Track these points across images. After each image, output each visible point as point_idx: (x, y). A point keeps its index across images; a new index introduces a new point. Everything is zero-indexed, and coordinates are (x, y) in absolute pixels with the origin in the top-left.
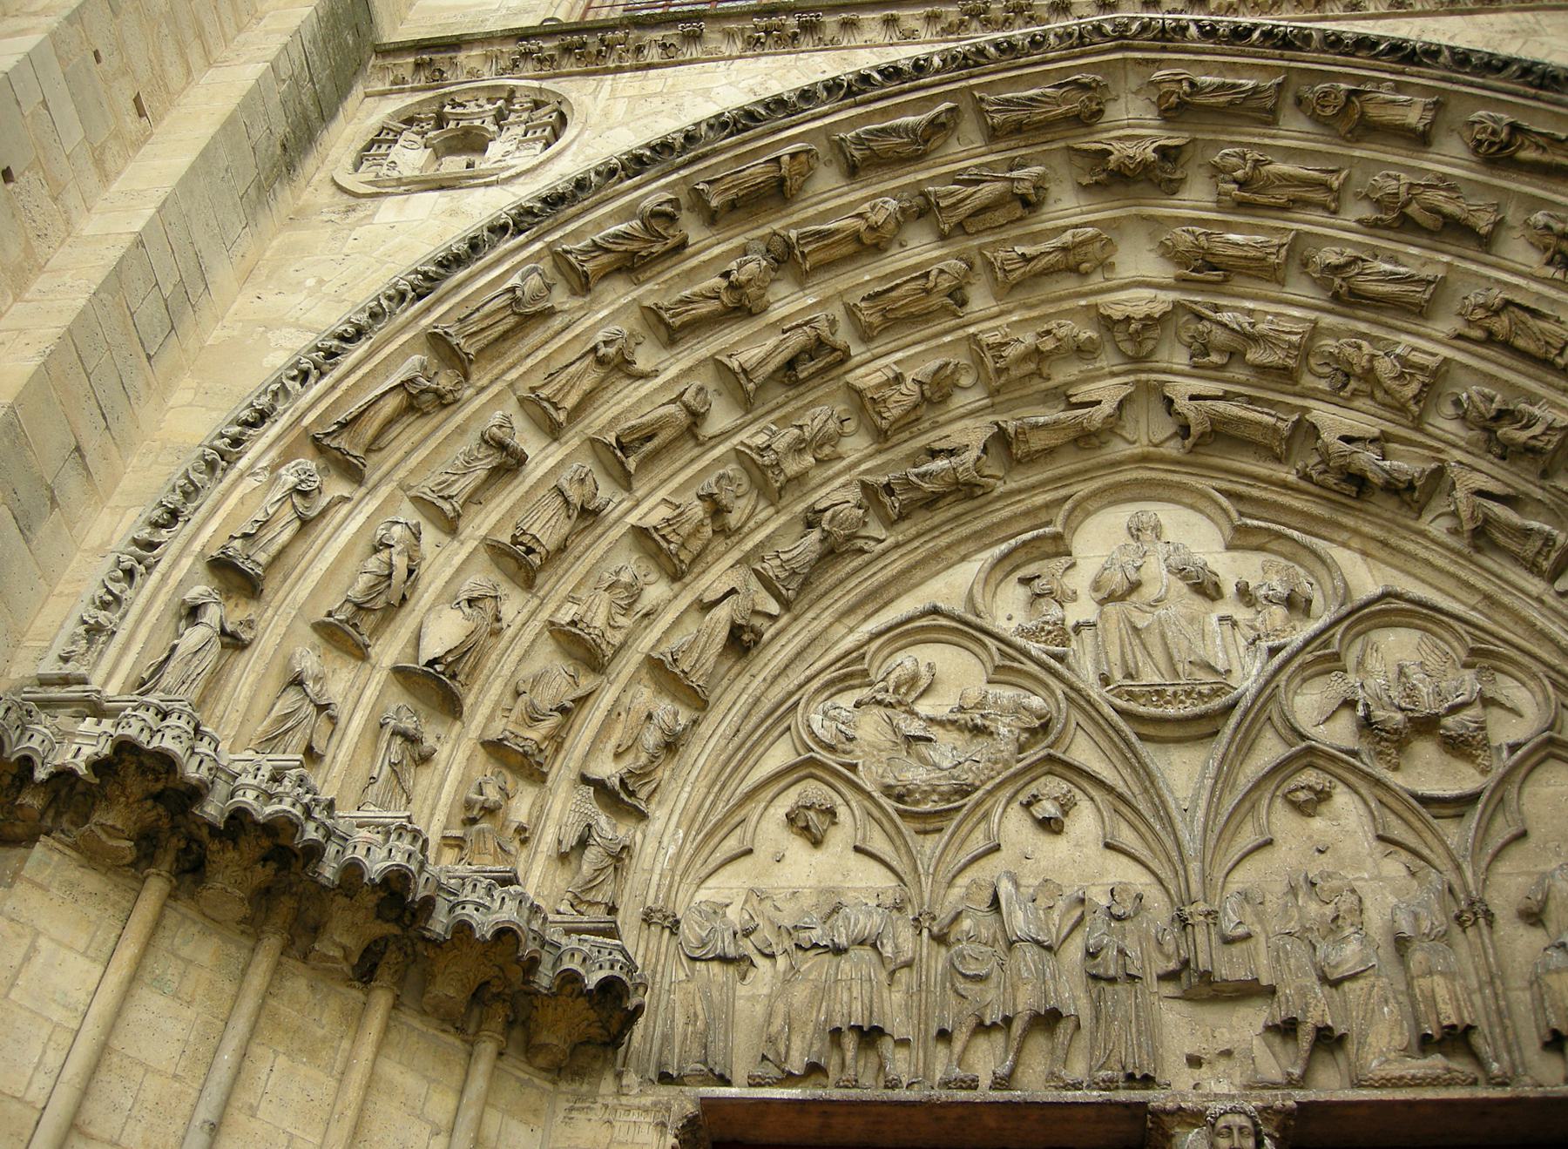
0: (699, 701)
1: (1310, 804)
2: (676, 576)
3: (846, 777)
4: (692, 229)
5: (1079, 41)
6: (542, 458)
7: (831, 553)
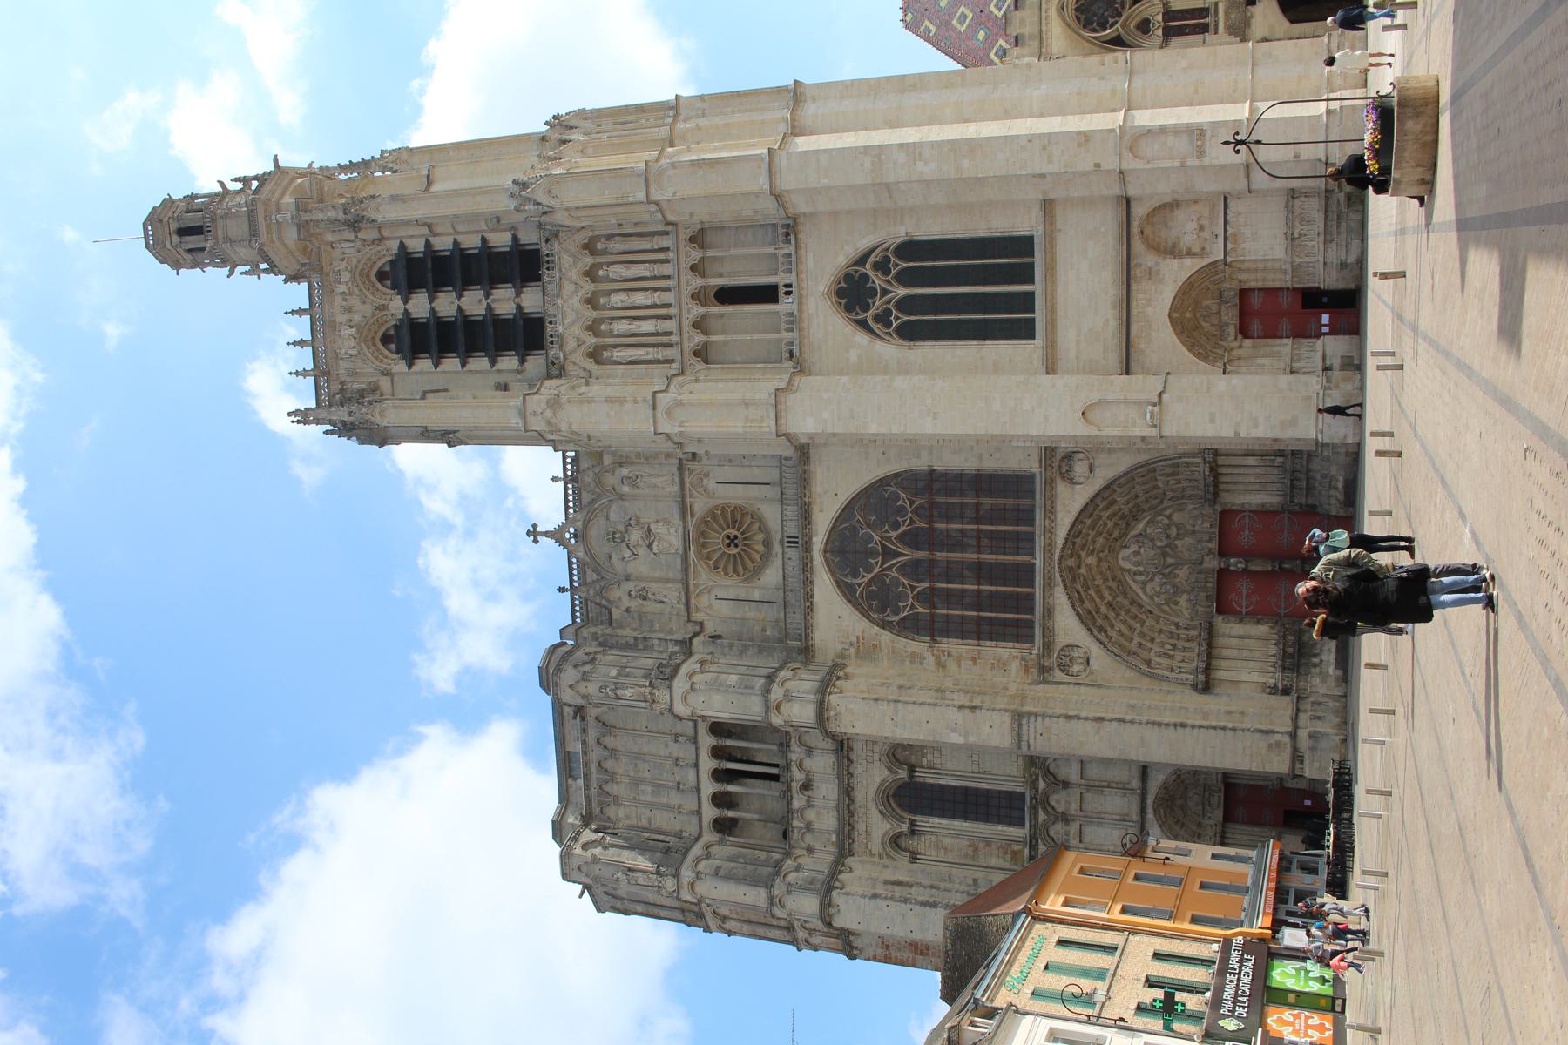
1: (1176, 546)
2: (1144, 622)
3: (1170, 599)
4: (1098, 624)
5: (1061, 571)
6: (1135, 642)
7: (1134, 602)
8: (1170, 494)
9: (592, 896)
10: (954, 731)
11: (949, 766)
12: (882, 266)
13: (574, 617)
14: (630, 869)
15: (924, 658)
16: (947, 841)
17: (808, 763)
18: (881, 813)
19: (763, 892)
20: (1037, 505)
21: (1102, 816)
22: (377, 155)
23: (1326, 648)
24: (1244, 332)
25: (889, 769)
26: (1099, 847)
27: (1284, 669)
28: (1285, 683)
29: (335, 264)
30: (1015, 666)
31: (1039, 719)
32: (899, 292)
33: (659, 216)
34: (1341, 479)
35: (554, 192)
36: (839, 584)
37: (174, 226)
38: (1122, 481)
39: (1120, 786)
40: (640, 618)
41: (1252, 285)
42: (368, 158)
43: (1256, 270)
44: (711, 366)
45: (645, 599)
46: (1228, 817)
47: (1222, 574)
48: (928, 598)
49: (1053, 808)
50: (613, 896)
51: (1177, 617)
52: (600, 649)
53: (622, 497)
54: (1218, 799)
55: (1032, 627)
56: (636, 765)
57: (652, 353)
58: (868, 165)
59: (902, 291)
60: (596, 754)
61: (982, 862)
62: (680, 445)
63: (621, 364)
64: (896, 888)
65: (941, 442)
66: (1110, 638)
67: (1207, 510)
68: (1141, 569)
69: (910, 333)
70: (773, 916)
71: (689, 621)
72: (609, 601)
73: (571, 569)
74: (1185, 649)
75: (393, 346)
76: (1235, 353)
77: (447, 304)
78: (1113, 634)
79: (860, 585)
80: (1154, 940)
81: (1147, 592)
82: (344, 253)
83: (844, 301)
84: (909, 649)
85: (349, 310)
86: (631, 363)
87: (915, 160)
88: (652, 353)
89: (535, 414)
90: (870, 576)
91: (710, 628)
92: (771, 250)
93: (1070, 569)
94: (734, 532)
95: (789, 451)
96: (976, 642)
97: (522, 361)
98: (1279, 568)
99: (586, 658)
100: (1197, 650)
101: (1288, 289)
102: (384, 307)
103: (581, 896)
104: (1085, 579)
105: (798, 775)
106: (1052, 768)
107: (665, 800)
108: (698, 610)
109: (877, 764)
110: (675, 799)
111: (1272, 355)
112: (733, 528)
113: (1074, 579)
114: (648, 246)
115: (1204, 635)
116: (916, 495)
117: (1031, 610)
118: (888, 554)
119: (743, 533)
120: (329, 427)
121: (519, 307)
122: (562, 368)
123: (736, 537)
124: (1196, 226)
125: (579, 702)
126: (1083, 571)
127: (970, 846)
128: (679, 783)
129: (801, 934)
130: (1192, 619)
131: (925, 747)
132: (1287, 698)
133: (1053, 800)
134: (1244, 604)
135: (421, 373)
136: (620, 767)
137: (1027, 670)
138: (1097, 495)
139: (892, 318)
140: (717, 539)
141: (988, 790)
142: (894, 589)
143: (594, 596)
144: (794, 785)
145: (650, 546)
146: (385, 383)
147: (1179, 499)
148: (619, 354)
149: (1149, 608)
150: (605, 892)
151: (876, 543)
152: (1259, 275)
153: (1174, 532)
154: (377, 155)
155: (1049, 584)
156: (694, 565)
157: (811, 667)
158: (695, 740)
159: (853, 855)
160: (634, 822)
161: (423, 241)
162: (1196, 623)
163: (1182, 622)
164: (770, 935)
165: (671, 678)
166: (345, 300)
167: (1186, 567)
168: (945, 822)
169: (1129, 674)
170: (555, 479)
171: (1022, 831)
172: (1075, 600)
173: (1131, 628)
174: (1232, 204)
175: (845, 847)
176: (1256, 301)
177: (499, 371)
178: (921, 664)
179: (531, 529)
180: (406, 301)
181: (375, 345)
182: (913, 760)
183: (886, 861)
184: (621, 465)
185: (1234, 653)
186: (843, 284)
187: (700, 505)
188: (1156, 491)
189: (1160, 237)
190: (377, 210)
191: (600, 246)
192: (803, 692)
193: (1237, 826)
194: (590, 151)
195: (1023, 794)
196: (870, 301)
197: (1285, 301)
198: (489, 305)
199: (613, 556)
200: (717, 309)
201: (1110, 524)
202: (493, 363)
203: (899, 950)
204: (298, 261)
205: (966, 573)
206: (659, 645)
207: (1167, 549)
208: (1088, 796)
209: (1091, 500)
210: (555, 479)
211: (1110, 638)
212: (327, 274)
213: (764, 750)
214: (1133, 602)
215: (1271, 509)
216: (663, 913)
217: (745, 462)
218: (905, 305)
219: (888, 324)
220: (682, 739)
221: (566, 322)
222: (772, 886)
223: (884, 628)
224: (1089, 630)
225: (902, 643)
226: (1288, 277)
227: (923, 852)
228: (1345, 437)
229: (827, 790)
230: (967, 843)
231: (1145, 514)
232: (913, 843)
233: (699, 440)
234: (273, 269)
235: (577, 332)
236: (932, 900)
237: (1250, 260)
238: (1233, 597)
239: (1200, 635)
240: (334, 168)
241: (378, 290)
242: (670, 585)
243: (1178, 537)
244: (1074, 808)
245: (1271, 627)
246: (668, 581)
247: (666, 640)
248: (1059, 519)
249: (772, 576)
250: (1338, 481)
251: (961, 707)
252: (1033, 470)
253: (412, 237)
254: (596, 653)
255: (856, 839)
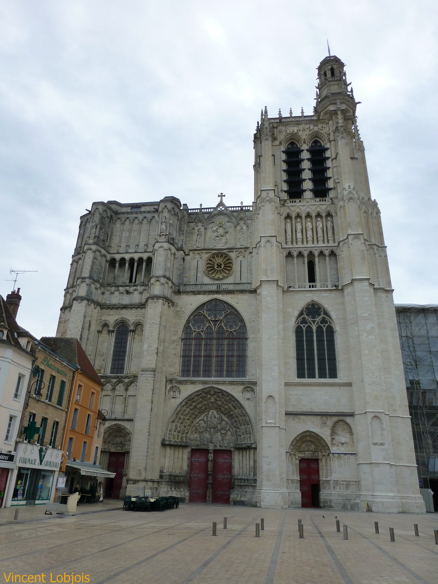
0: (190, 426)
1: (217, 433)
3: (197, 430)
5: (209, 387)
6: (182, 417)
7: (196, 416)
8: (238, 430)
9: (87, 215)
10: (148, 346)
11: (134, 345)
12: (324, 321)
13: (191, 209)
14: (96, 227)
15: (176, 336)
16: (106, 345)
17: (136, 293)
18: (117, 320)
19: (87, 275)
20: (234, 378)
21: (114, 404)
22: (361, 140)
23: (178, 493)
24: (302, 461)
25: (134, 323)
26: (101, 402)
27: (170, 476)
28: (164, 476)
29: (321, 125)
30: (172, 370)
31: (153, 379)
32: (314, 327)
33: (341, 239)
34: (245, 499)
35: (351, 200)
36: (203, 305)
37: (335, 67)
38: (244, 412)
39: (125, 411)
40: (190, 233)
41: (320, 464)
42: (360, 136)
43: (326, 466)
44: (285, 258)
45: (198, 235)
46: (112, 454)
47: (207, 451)
48: (199, 338)
49: (117, 385)
50: (86, 222)
51: (191, 433)
52: (179, 218)
53: (235, 227)
54: (119, 450)
55: (187, 376)
56: (136, 231)
57: (289, 237)
58: (365, 315)
59: (314, 328)
60: (140, 217)
61: (97, 358)
62: (256, 247)
63: (285, 226)
64: (88, 325)
65: (258, 342)
66: (182, 407)
67: (232, 445)
68: (209, 419)
69: (298, 331)
70: (78, 279)
71: (190, 250)
72: (196, 223)
73: (209, 208)
74: (178, 436)
75: (290, 146)
76: (294, 456)
77: (306, 165)
78: (184, 408)
79: (203, 312)
80: (63, 422)
81: (200, 421)
82: (325, 128)
83: (310, 307)
84: (179, 330)
85: (304, 130)
86: (286, 230)
87: (368, 333)
88: (289, 237)
89: (268, 194)
90: (207, 316)
91: (187, 258)
92: (329, 279)
93: (210, 391)
94: (223, 267)
95: (254, 286)
96: (182, 355)
97: (285, 192)
98: (210, 474)
99: (176, 212)
100: (178, 440)
101: (319, 478)
102: (305, 143)
103: (86, 210)
104: (206, 397)
105: (131, 289)
106: (133, 384)
107: (123, 241)
108: (194, 253)
109: (136, 318)
110: (123, 245)
111: (293, 472)
112: (224, 266)
113: (206, 393)
114: (329, 236)
115: (183, 444)
116: (237, 333)
117: (194, 376)
118: (215, 321)
119: (222, 270)
120: (260, 123)
121: (305, 191)
122: (284, 205)
123: (220, 267)
124: (343, 442)
125: (160, 209)
126: (209, 396)
127: (104, 353)
128: (129, 246)
129: (70, 291)
130: (190, 439)
131: (142, 336)
132: (159, 478)
133: (121, 385)
134: (195, 460)
135: (280, 155)
136: (136, 226)
137: (170, 374)
138: (238, 401)
139: (304, 324)
140: (219, 260)
141: (125, 360)
142: (202, 324)
143: (199, 217)
144: (128, 287)
145: (217, 236)
146: (277, 143)
147: (236, 434)
148: (289, 225)
149: (194, 422)
150: (88, 219)
151: (219, 318)
152: (324, 467)
153: (223, 432)
154: (361, 140)
155: (204, 383)
156: (210, 252)
157: (172, 294)
158: (145, 252)
159: (101, 309)
160: (115, 230)
161: (330, 156)
162: (188, 441)
163: (189, 435)
164: (70, 279)
165: (168, 242)
166: (307, 129)
167: (210, 437)
168: (113, 344)
169: (169, 414)
170: (242, 203)
171: (109, 373)
172: (198, 393)
173: (187, 414)
174: (353, 457)
175: (103, 306)
176: (313, 466)
177: (282, 183)
178: (174, 335)
179: (223, 195)
180: (307, 150)
181: (291, 139)
182: (137, 332)
183: (99, 321)
184: (247, 226)
185: (176, 455)
186: (316, 306)
187: (233, 255)
188: (239, 424)
189: (339, 427)
190: (343, 137)
191: (329, 218)
192: (163, 290)
193: (108, 458)
194: (365, 215)
195: (123, 373)
196: (310, 316)
197: (314, 477)
198: (306, 179)
199: (213, 224)
200: (306, 260)
201: (226, 407)
202: (285, 181)
203: (64, 327)
204: (322, 111)
205: (208, 352)
206: (181, 239)
207: (216, 429)
208: (122, 398)
209: (236, 399)
210: (242, 203)
211: (182, 407)
212: (317, 122)
213: (141, 278)
214: (196, 416)
215: (232, 471)
216: (80, 240)
217: (249, 271)
218: (309, 329)
219: (302, 323)
220: (146, 247)
221: (300, 206)
222: (90, 279)
223: (187, 321)
224: (186, 398)
225: (181, 327)
226: (324, 479)
227: (102, 335)
228: (263, 501)
229: (126, 300)
230: (104, 352)
231: (230, 420)
232: (105, 332)
233: (258, 253)
234: (318, 103)
235: (297, 210)
236: (83, 338)
237: (330, 463)
238: (198, 455)
239: (184, 442)
240: (356, 124)
241: (311, 140)
242: (203, 244)
243: (221, 433)
244: (117, 393)
245: (186, 471)
246: (204, 243)
247: (183, 242)
248: (228, 386)
249: (207, 280)
250: (244, 498)
251: (158, 349)
252: (247, 377)
253: (331, 152)
254: (178, 216)
255: (107, 310)
